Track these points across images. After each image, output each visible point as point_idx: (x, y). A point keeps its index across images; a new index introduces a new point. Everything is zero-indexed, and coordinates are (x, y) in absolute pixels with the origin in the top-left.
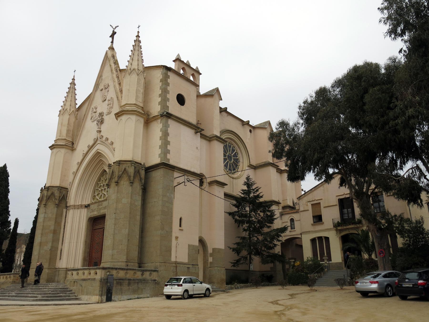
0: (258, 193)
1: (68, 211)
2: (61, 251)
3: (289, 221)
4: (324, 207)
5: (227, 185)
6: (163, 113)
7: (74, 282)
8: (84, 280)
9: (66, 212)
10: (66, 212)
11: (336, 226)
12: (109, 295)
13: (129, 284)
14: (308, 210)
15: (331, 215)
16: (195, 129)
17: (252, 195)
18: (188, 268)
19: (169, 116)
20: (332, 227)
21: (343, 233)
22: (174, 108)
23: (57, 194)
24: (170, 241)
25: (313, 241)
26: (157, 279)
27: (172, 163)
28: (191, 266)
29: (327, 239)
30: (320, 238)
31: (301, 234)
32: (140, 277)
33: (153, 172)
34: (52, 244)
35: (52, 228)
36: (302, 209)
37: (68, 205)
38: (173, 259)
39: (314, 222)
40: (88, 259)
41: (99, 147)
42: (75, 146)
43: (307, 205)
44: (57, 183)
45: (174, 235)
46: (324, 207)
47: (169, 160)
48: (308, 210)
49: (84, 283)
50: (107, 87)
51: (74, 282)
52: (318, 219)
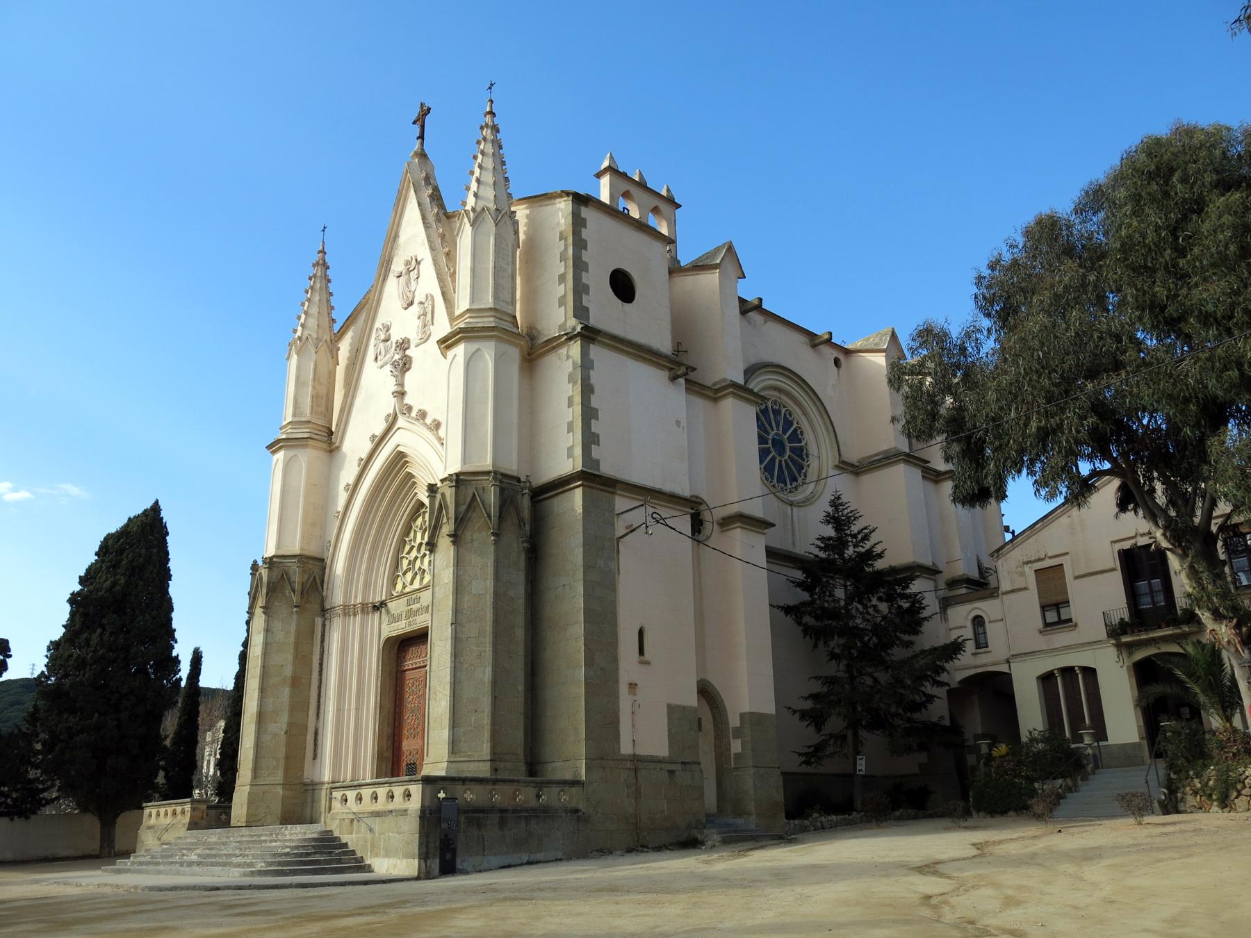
0: (868, 545)
1: (327, 623)
2: (316, 733)
3: (969, 624)
4: (1076, 578)
5: (773, 525)
7: (352, 820)
8: (377, 814)
9: (324, 626)
10: (324, 626)
11: (1116, 631)
12: (448, 856)
13: (502, 824)
14: (1026, 589)
15: (1101, 598)
16: (671, 369)
17: (850, 552)
18: (671, 772)
19: (589, 335)
20: (1104, 635)
21: (1140, 655)
22: (607, 311)
23: (297, 576)
24: (614, 696)
25: (1047, 679)
26: (580, 806)
27: (606, 469)
28: (679, 767)
29: (1090, 672)
30: (1068, 672)
31: (1008, 661)
32: (533, 803)
33: (555, 500)
34: (291, 715)
35: (288, 671)
36: (1005, 585)
37: (327, 606)
38: (626, 749)
39: (1046, 625)
40: (388, 754)
43: (1022, 574)
44: (295, 547)
45: (624, 678)
46: (1076, 578)
47: (597, 462)
48: (1026, 589)
49: (376, 824)
50: (414, 265)
51: (352, 820)
52: (1055, 610)
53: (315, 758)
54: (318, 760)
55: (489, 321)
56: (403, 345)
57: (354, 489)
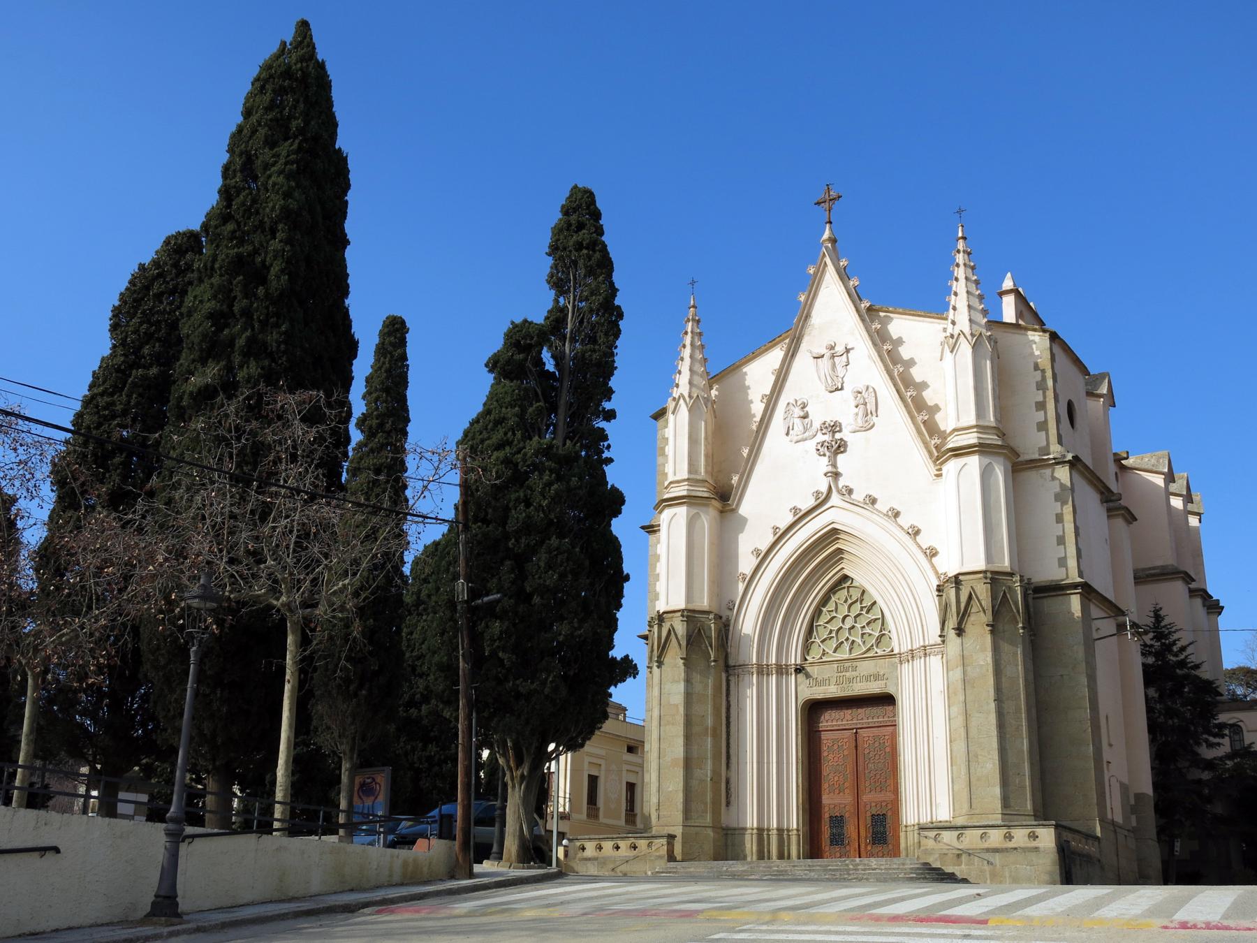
1: (731, 678)
2: (728, 782)
6: (1064, 456)
7: (959, 856)
8: (996, 850)
9: (728, 682)
10: (728, 682)
16: (1102, 493)
33: (1045, 601)
37: (731, 662)
38: (1109, 816)
41: (837, 515)
42: (732, 502)
49: (997, 859)
51: (959, 856)
53: (728, 804)
54: (733, 808)
55: (993, 439)
56: (834, 428)
57: (764, 557)
